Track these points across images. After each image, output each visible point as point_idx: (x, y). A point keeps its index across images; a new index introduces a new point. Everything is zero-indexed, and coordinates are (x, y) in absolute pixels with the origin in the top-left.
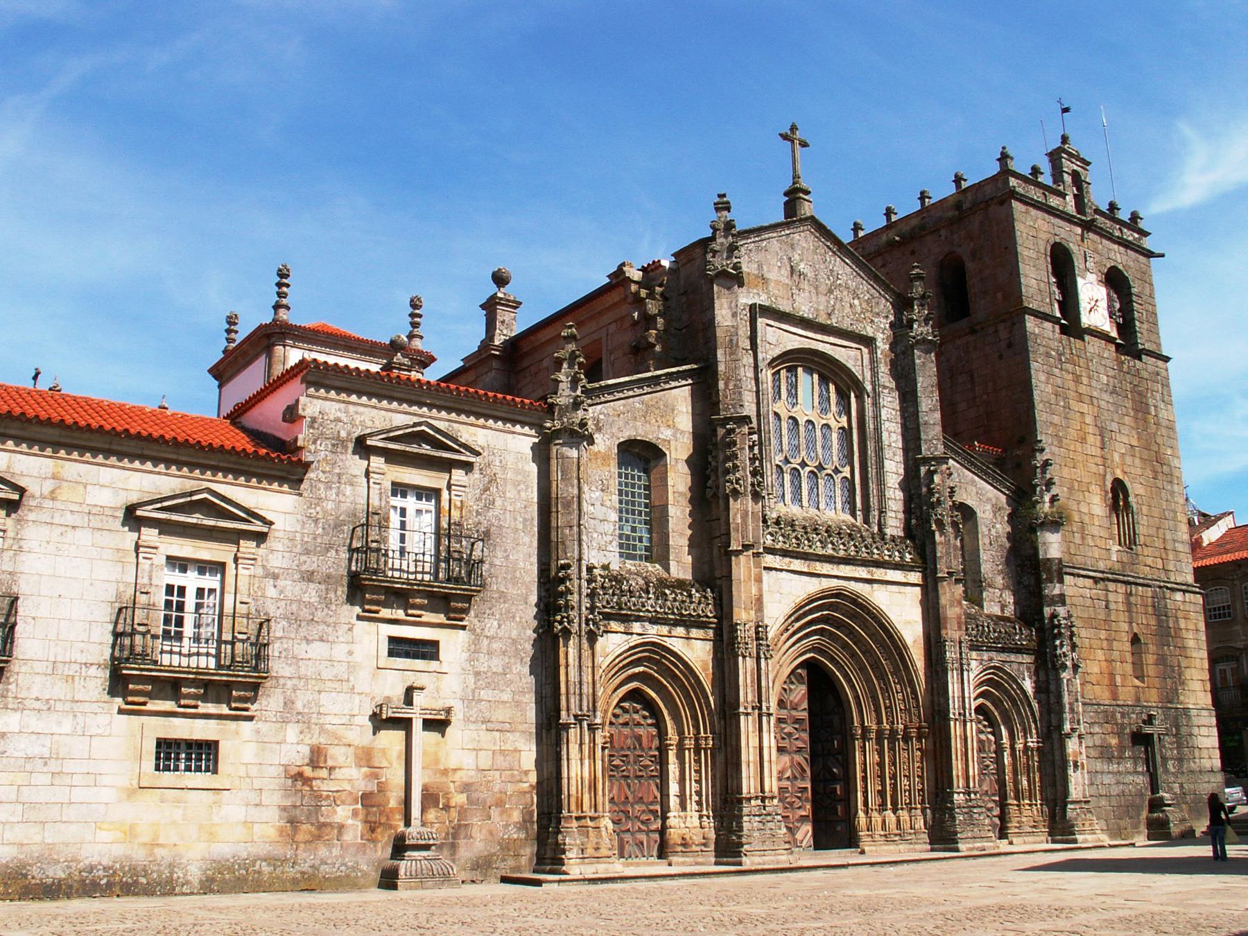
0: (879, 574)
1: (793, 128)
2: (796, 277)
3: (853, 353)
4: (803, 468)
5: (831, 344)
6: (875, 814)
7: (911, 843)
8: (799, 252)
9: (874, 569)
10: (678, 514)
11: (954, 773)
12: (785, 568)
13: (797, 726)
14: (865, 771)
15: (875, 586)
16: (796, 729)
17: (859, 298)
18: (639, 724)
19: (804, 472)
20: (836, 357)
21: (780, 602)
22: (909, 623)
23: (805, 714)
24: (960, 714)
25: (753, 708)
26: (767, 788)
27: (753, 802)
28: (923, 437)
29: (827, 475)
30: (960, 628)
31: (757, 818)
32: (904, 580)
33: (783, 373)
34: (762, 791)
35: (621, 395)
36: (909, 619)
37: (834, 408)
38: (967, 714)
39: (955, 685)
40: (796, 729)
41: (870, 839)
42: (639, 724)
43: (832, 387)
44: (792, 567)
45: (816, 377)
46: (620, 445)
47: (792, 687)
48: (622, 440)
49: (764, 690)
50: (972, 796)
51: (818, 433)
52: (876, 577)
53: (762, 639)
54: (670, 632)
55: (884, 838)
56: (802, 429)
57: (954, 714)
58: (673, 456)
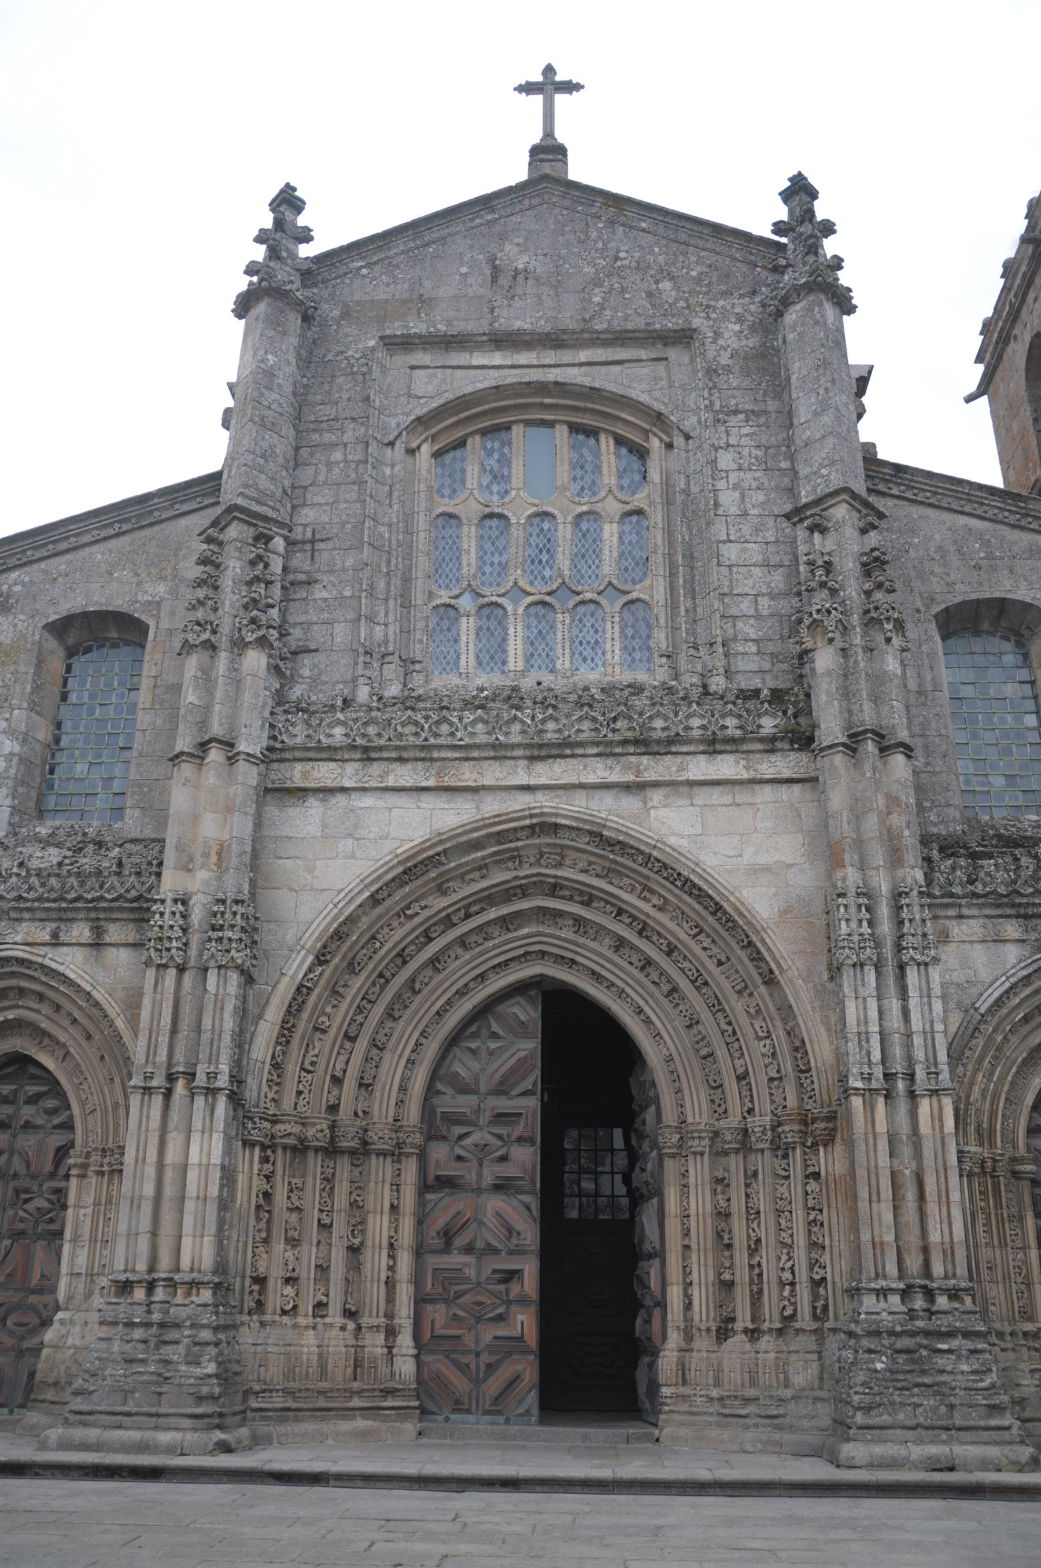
0: (654, 769)
1: (549, 70)
2: (504, 281)
3: (644, 371)
4: (516, 603)
5: (582, 364)
6: (702, 1343)
7: (779, 1428)
8: (521, 241)
9: (645, 760)
10: (159, 722)
11: (865, 1236)
12: (374, 784)
13: (503, 1131)
14: (687, 1233)
15: (656, 797)
16: (499, 1137)
17: (672, 278)
18: (28, 1126)
19: (516, 609)
20: (596, 385)
21: (353, 856)
22: (767, 869)
23: (532, 1104)
24: (888, 1076)
25: (171, 1078)
26: (185, 1262)
27: (140, 1294)
28: (803, 471)
29: (583, 602)
30: (895, 858)
31: (138, 1334)
32: (745, 775)
33: (475, 442)
34: (177, 1270)
35: (63, 546)
36: (764, 859)
37: (609, 479)
38: (920, 1074)
39: (873, 1005)
40: (499, 1137)
41: (685, 1408)
42: (28, 1126)
43: (606, 443)
44: (391, 782)
45: (561, 432)
46: (60, 628)
47: (493, 1045)
48: (53, 618)
49: (206, 1037)
50: (942, 1302)
51: (565, 532)
52: (650, 776)
53: (221, 928)
54: (55, 935)
55: (716, 1408)
56: (517, 533)
57: (869, 1078)
58: (164, 624)
